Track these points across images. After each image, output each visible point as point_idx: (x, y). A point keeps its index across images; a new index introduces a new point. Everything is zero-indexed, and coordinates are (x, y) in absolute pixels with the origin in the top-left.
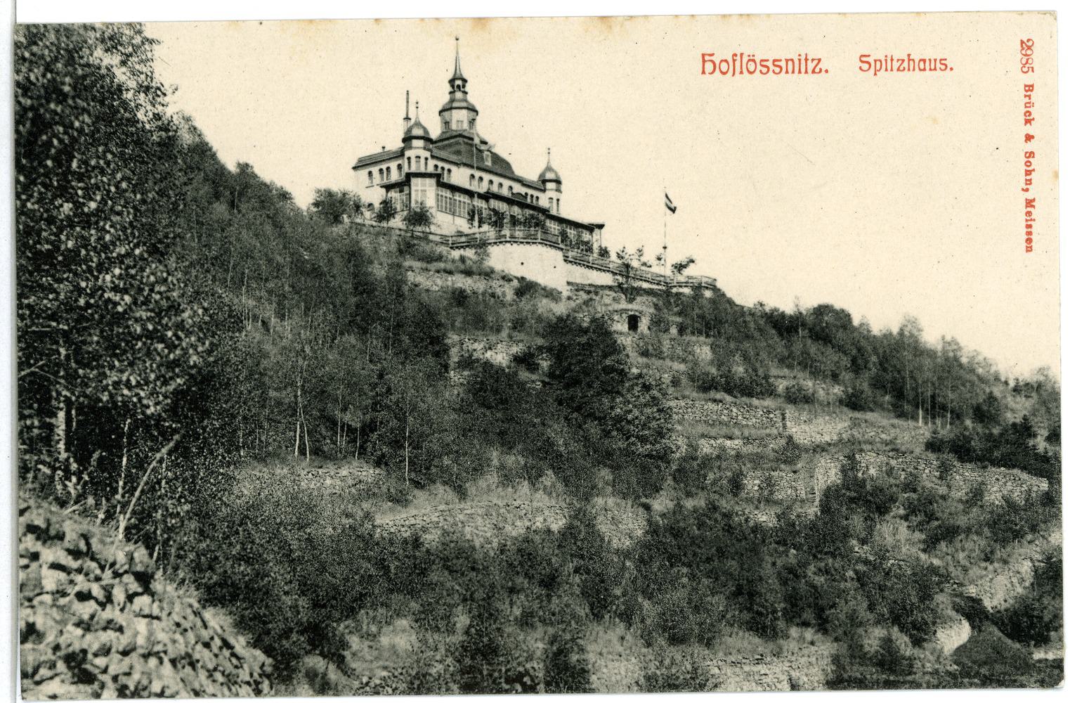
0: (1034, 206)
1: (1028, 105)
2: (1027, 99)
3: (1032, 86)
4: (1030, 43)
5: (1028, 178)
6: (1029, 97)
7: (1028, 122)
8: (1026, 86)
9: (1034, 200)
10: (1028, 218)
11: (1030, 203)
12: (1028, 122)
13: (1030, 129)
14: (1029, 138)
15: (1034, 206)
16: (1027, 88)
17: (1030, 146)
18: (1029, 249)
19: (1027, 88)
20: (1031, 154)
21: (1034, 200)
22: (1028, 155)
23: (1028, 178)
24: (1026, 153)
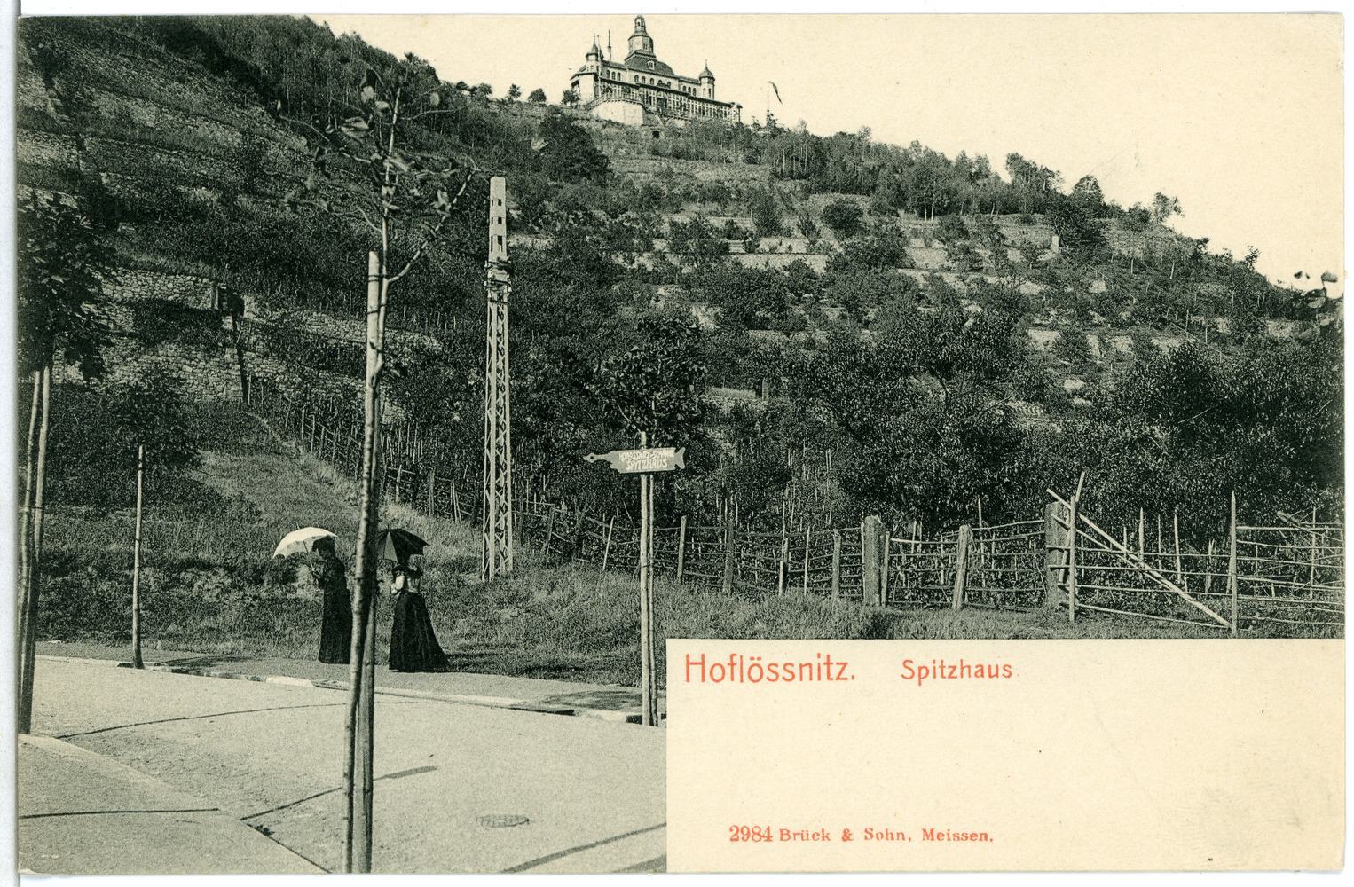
0: (932, 831)
1: (805, 837)
2: (798, 837)
3: (781, 831)
4: (735, 830)
6: (795, 834)
7: (825, 837)
8: (782, 839)
9: (924, 831)
10: (946, 837)
11: (929, 835)
12: (825, 837)
13: (836, 836)
14: (846, 836)
15: (932, 831)
16: (785, 837)
17: (858, 834)
18: (985, 836)
19: (785, 837)
20: (869, 833)
21: (924, 831)
22: (869, 836)
23: (895, 836)
24: (866, 838)
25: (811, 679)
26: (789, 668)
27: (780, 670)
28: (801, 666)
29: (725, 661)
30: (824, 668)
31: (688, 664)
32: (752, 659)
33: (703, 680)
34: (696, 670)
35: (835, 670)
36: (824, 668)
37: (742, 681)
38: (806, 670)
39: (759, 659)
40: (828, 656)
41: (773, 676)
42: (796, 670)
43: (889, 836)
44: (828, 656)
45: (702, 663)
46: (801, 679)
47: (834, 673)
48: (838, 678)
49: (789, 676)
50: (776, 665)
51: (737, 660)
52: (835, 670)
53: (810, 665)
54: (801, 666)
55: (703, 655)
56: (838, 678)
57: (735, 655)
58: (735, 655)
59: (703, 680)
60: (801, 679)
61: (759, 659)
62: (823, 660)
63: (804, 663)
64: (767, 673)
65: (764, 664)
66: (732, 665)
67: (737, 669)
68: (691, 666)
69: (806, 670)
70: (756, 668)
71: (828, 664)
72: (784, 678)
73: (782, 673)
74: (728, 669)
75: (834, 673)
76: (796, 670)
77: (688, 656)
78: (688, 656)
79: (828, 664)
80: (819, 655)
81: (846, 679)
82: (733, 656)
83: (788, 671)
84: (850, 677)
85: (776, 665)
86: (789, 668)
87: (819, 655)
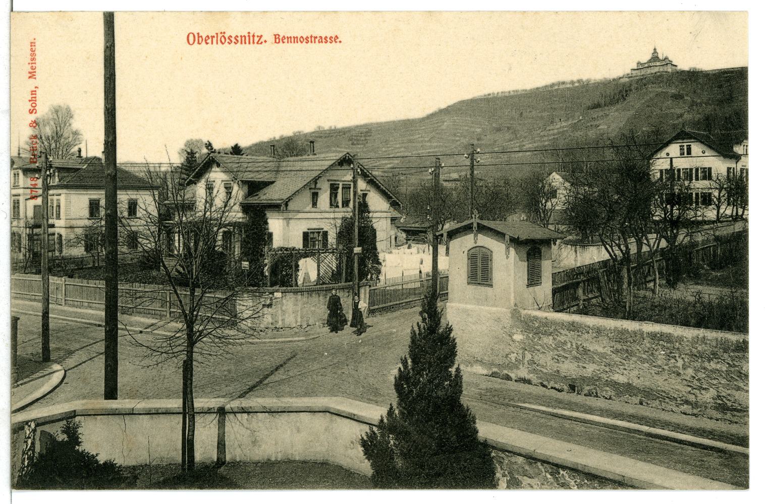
0: (30, 73)
5: (33, 96)
9: (30, 77)
15: (30, 73)
21: (30, 77)
23: (33, 96)
30: (251, 38)
35: (256, 39)
36: (251, 38)
37: (217, 43)
42: (239, 39)
43: (33, 99)
47: (256, 41)
48: (257, 43)
52: (256, 39)
53: (245, 36)
56: (257, 43)
61: (224, 33)
62: (251, 35)
71: (254, 36)
75: (256, 41)
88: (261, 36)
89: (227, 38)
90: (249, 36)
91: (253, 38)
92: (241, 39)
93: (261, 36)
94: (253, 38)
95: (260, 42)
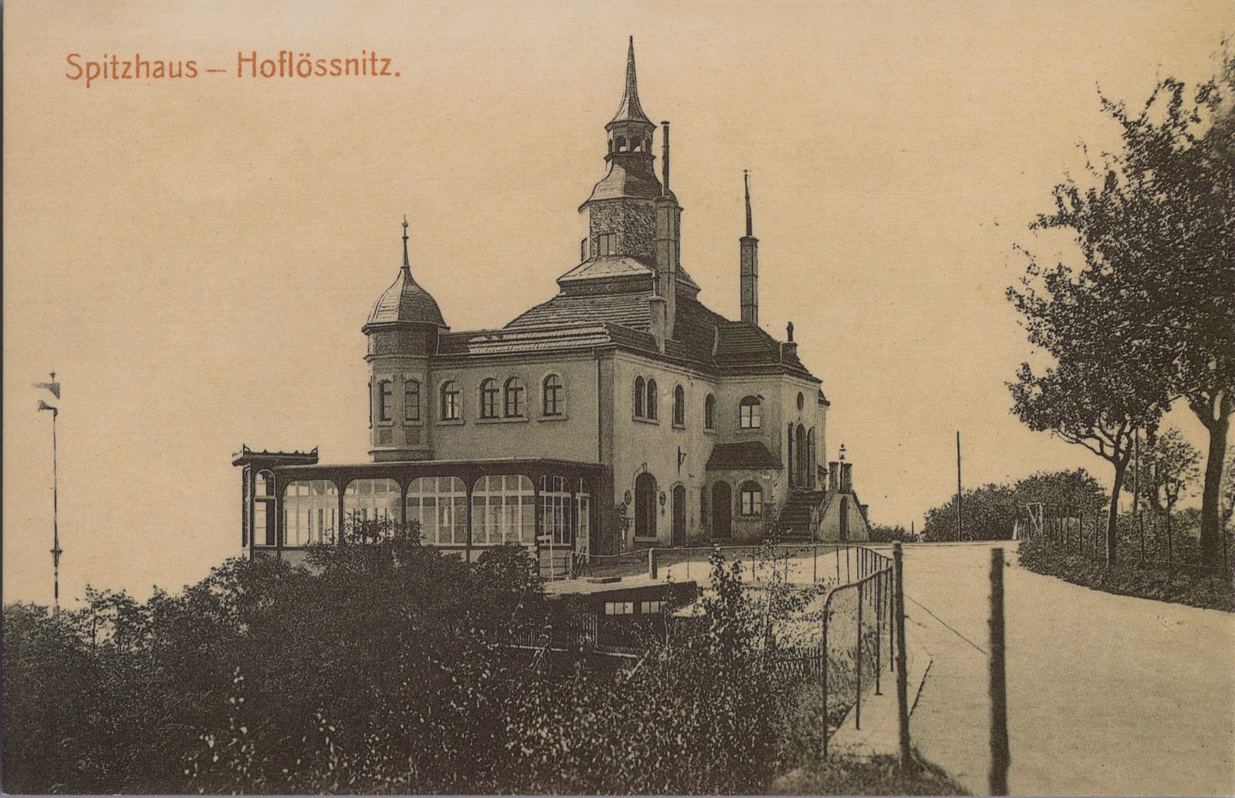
25: (357, 73)
26: (336, 63)
27: (327, 65)
28: (348, 62)
29: (276, 59)
30: (369, 64)
31: (241, 59)
32: (302, 55)
33: (254, 75)
34: (247, 67)
35: (379, 66)
36: (369, 64)
38: (352, 66)
39: (308, 55)
40: (373, 53)
41: (321, 71)
42: (343, 66)
44: (373, 53)
45: (254, 60)
46: (347, 73)
48: (383, 73)
49: (335, 71)
50: (324, 61)
51: (286, 57)
52: (379, 66)
53: (356, 61)
54: (348, 62)
55: (254, 54)
56: (383, 73)
57: (285, 52)
58: (285, 52)
59: (254, 75)
60: (347, 73)
61: (308, 55)
62: (368, 56)
63: (350, 58)
64: (315, 69)
65: (312, 59)
66: (282, 61)
67: (286, 65)
68: (243, 64)
69: (352, 66)
70: (305, 63)
71: (373, 60)
72: (331, 73)
73: (330, 68)
74: (278, 65)
76: (343, 66)
77: (240, 53)
78: (240, 53)
79: (373, 60)
80: (364, 52)
81: (389, 74)
82: (283, 53)
83: (333, 66)
84: (393, 74)
85: (324, 61)
86: (336, 63)
87: (364, 52)
88: (388, 61)
89: (314, 65)
90: (364, 60)
91: (373, 65)
92: (347, 65)
93: (388, 61)
94: (373, 65)
95: (386, 72)
